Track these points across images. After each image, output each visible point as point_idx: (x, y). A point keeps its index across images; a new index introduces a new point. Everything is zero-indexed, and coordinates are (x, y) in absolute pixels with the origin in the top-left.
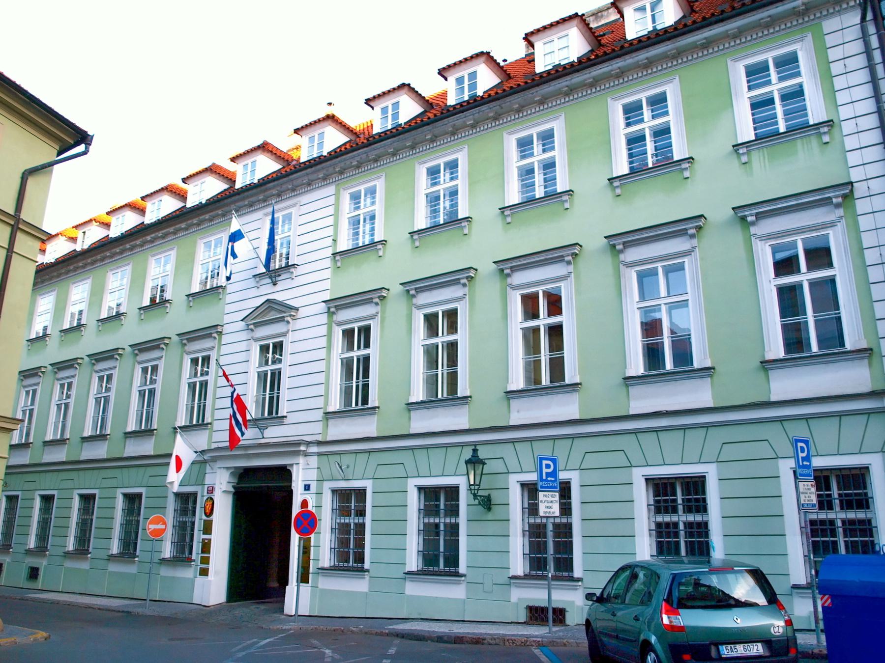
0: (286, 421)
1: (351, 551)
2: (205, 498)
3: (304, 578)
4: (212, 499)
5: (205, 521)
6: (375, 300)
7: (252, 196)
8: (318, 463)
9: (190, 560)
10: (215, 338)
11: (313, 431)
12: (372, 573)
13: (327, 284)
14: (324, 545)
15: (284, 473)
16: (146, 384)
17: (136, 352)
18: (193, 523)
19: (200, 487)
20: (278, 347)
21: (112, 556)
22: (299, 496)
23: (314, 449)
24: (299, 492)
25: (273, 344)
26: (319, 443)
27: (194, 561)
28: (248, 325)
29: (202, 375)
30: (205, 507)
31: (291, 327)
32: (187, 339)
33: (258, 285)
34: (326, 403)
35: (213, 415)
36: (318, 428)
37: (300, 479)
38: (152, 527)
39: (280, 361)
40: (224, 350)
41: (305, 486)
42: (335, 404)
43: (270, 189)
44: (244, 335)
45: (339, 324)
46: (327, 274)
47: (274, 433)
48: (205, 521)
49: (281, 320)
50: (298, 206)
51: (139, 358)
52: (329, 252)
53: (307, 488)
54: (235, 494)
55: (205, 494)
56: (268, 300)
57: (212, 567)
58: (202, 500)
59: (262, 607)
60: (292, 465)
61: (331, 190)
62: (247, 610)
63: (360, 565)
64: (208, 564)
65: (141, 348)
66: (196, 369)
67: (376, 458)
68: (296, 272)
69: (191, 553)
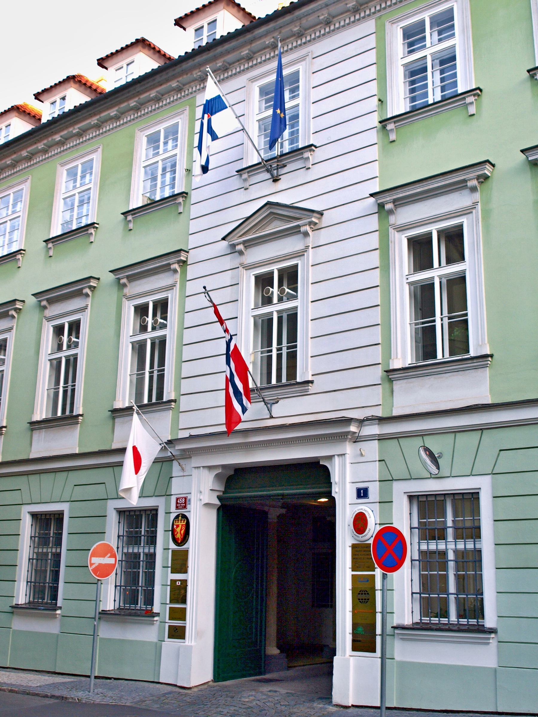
0: (312, 389)
1: (452, 598)
2: (173, 516)
3: (363, 642)
4: (184, 517)
5: (174, 551)
6: (470, 184)
7: (228, 52)
8: (381, 451)
9: (151, 614)
10: (175, 271)
11: (367, 401)
12: (502, 635)
13: (374, 169)
15: (317, 473)
16: (60, 348)
17: (44, 303)
18: (151, 558)
19: (163, 499)
20: (290, 276)
21: (17, 607)
23: (374, 430)
24: (348, 501)
25: (280, 271)
26: (381, 420)
27: (158, 614)
28: (233, 246)
30: (173, 531)
31: (311, 241)
32: (128, 277)
33: (246, 185)
34: (388, 354)
35: (178, 387)
36: (375, 396)
37: (348, 479)
38: (97, 561)
39: (295, 297)
40: (192, 287)
41: (359, 490)
42: (404, 354)
43: (260, 37)
44: (228, 262)
45: (401, 229)
46: (373, 153)
47: (291, 409)
48: (174, 551)
49: (295, 231)
50: (309, 59)
51: (48, 313)
52: (374, 120)
53: (362, 493)
54: (218, 510)
55: (173, 508)
56: (268, 203)
57: (190, 624)
58: (166, 520)
59: (282, 689)
60: (330, 458)
61: (370, 26)
62: (267, 695)
63: (473, 621)
64: (185, 620)
65: (50, 297)
68: (313, 157)
69: (149, 601)
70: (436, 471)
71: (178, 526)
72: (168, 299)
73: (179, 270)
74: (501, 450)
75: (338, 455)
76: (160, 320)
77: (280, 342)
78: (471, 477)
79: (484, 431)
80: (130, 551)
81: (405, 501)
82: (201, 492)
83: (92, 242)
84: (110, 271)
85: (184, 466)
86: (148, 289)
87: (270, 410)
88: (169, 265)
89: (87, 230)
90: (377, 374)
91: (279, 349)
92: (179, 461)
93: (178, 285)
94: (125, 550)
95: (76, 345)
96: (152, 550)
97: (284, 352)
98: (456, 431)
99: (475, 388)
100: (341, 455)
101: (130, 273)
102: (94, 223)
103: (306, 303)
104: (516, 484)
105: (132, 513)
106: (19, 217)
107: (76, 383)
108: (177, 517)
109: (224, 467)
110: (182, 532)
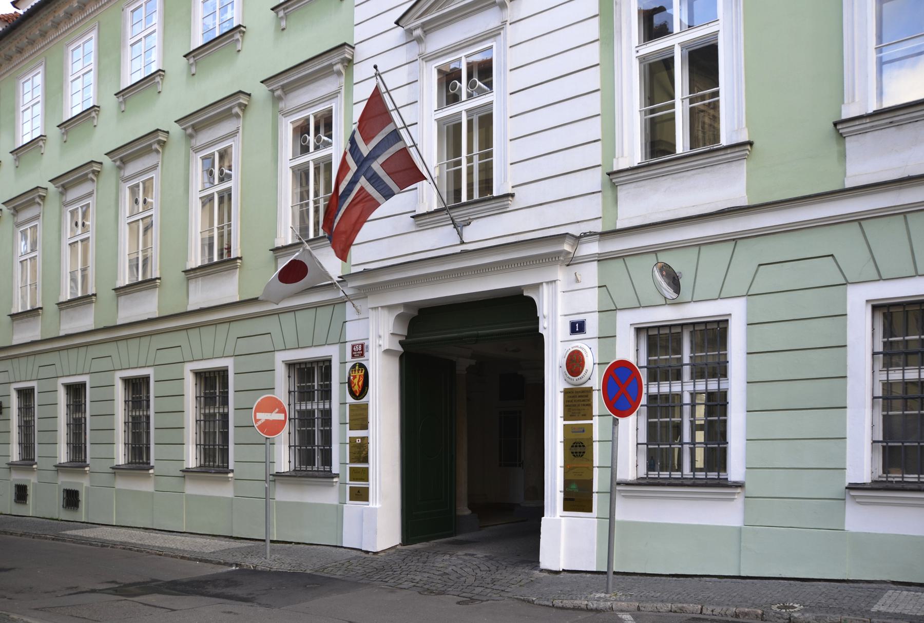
0: (513, 204)
2: (349, 366)
4: (362, 366)
8: (601, 276)
14: (624, 443)
18: (327, 416)
22: (559, 345)
23: (592, 248)
24: (560, 337)
29: (317, 148)
32: (283, 87)
37: (560, 311)
47: (485, 230)
53: (578, 328)
54: (402, 358)
58: (342, 371)
60: (537, 286)
66: (305, 140)
67: (749, 255)
70: (674, 296)
71: (355, 377)
72: (331, 110)
73: (343, 72)
74: (760, 265)
75: (547, 283)
76: (324, 138)
77: (470, 150)
78: (719, 301)
79: (739, 242)
80: (303, 407)
81: (632, 333)
82: (380, 337)
83: (239, 51)
84: (262, 82)
85: (359, 308)
86: (307, 101)
87: (460, 234)
88: (331, 65)
89: (233, 36)
90: (595, 180)
91: (470, 160)
92: (354, 302)
93: (343, 91)
94: (298, 408)
95: (229, 177)
96: (327, 406)
97: (476, 163)
98: (699, 244)
99: (724, 187)
100: (551, 282)
101: (285, 82)
102: (239, 26)
103: (499, 99)
104: (780, 307)
105: (303, 366)
106: (154, 31)
107: (232, 222)
108: (354, 367)
109: (406, 305)
110: (360, 383)
